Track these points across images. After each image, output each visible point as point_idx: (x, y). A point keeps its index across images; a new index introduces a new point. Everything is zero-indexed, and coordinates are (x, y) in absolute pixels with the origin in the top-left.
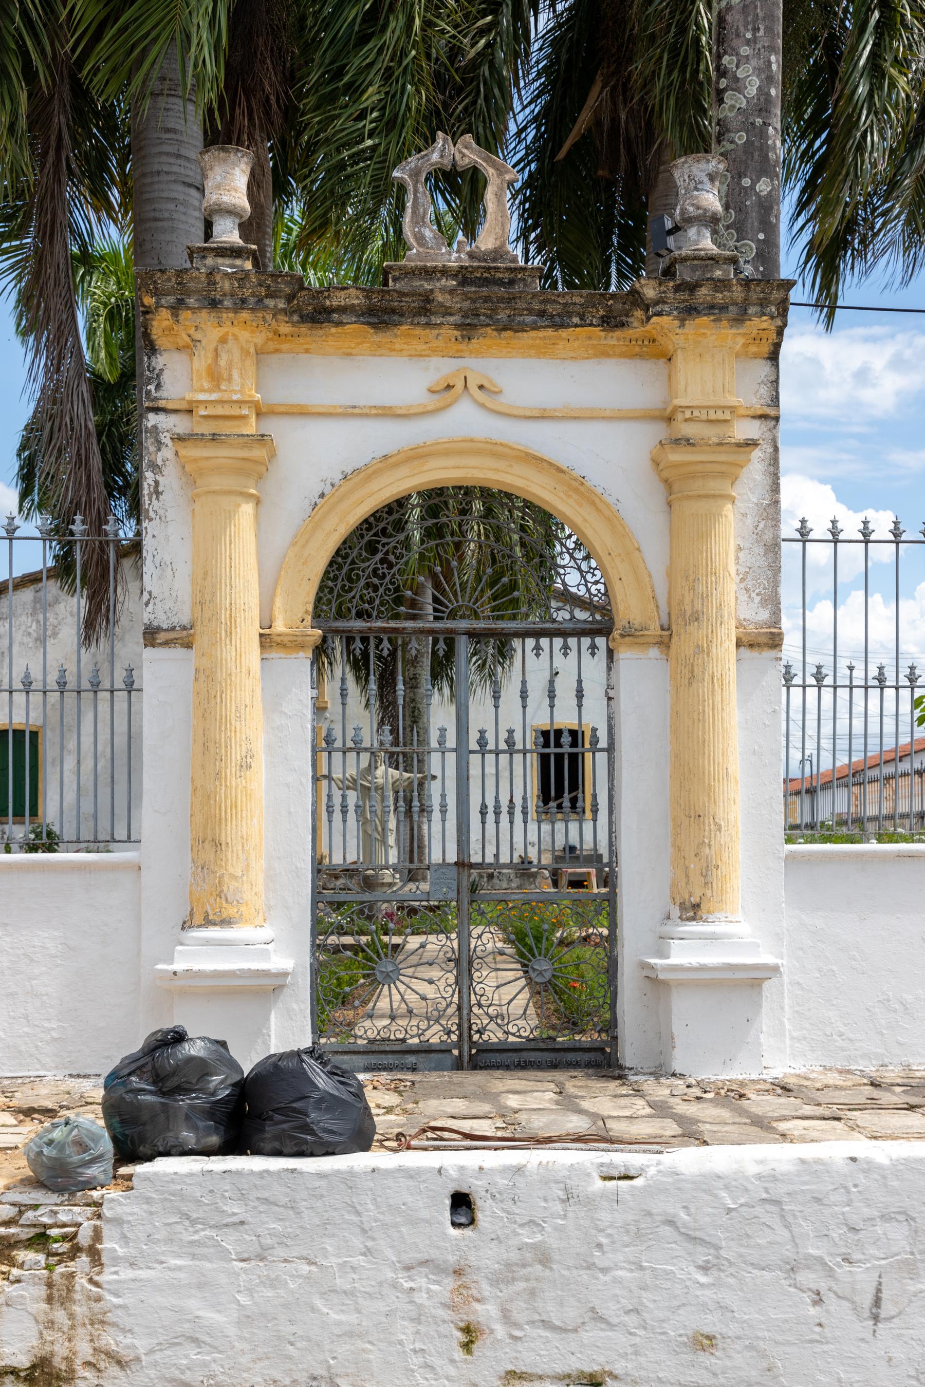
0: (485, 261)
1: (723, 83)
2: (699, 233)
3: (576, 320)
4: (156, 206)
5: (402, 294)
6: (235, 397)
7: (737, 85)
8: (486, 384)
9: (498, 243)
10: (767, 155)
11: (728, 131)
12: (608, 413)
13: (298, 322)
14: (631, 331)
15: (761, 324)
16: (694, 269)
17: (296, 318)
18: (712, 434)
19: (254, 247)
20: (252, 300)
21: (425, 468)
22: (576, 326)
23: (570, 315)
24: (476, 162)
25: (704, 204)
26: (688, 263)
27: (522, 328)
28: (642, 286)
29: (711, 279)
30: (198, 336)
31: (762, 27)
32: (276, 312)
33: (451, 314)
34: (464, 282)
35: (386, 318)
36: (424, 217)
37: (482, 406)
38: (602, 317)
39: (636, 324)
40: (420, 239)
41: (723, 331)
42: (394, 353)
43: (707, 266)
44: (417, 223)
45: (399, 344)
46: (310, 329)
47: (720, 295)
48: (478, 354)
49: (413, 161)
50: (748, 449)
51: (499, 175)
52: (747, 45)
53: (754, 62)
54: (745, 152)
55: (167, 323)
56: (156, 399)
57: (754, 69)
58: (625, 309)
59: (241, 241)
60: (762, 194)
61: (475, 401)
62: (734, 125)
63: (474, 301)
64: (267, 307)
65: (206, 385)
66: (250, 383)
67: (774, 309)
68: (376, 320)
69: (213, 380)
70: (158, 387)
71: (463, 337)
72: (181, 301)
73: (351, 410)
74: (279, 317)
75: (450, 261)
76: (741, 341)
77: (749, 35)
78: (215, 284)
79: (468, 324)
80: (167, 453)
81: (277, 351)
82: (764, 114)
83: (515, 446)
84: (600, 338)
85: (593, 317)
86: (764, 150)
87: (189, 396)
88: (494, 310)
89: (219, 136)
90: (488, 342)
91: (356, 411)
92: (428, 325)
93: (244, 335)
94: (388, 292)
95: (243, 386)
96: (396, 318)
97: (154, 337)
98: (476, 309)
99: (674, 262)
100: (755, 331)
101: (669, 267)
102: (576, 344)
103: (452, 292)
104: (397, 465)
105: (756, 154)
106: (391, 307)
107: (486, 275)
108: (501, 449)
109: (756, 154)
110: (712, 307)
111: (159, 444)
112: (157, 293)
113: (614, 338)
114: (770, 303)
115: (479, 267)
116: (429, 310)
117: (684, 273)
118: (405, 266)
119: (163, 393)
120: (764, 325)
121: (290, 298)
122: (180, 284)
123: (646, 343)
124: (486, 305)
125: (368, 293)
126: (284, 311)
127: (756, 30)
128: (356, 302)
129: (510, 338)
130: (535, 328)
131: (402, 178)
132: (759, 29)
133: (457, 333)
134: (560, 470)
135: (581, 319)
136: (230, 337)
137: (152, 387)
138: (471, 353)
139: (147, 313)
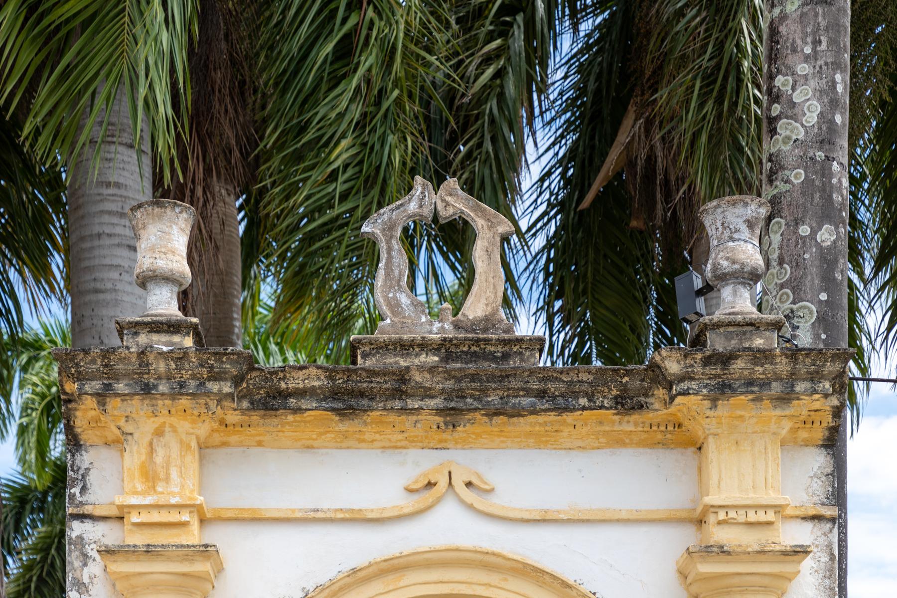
0: (474, 331)
1: (776, 109)
2: (735, 293)
3: (583, 401)
4: (97, 275)
5: (371, 373)
6: (173, 501)
7: (793, 110)
8: (475, 481)
9: (489, 309)
10: (831, 197)
11: (782, 168)
12: (624, 515)
13: (248, 409)
14: (651, 415)
15: (815, 404)
16: (729, 337)
17: (245, 404)
18: (750, 539)
19: (195, 320)
20: (193, 384)
21: (402, 584)
22: (584, 408)
23: (576, 395)
24: (462, 212)
25: (741, 257)
26: (722, 330)
27: (517, 413)
28: (663, 359)
29: (749, 349)
30: (129, 428)
31: (824, 39)
32: (222, 398)
33: (432, 397)
34: (448, 357)
35: (353, 402)
36: (399, 280)
37: (471, 507)
38: (616, 397)
39: (657, 406)
40: (395, 306)
41: (764, 413)
42: (363, 445)
43: (744, 333)
44: (391, 287)
45: (369, 433)
46: (263, 417)
47: (760, 369)
48: (464, 444)
49: (386, 213)
50: (796, 558)
51: (489, 228)
52: (806, 62)
53: (814, 83)
54: (803, 194)
55: (93, 413)
56: (81, 504)
57: (815, 91)
58: (642, 387)
59: (180, 314)
60: (825, 244)
61: (462, 502)
62: (789, 161)
63: (459, 380)
64: (208, 393)
65: (139, 487)
66: (192, 482)
67: (827, 385)
68: (341, 405)
69: (147, 480)
70: (84, 489)
71: (446, 423)
72: (108, 387)
73: (312, 515)
74: (225, 403)
75: (430, 332)
76: (787, 425)
77: (808, 50)
78: (148, 365)
79: (453, 409)
80: (95, 568)
81: (224, 444)
82: (827, 146)
83: (511, 556)
84: (613, 422)
85: (604, 397)
86: (827, 190)
87: (119, 500)
88: (484, 391)
89: (165, 191)
90: (477, 429)
91: (319, 515)
92: (404, 410)
93: (184, 426)
94: (355, 371)
95: (182, 486)
96: (365, 402)
97: (78, 430)
98: (461, 389)
99: (705, 327)
100: (805, 413)
101: (698, 336)
102: (585, 430)
103: (432, 370)
104: (367, 579)
105: (817, 196)
106: (359, 391)
107: (474, 348)
108: (493, 559)
109: (817, 196)
110: (750, 383)
111: (85, 556)
112: (80, 378)
113: (631, 424)
114: (823, 377)
115: (466, 339)
116: (405, 393)
117: (716, 343)
118: (377, 340)
119: (89, 497)
120: (817, 405)
121: (237, 380)
122: (106, 366)
123: (670, 428)
124: (474, 385)
125: (331, 374)
126: (230, 396)
127: (816, 42)
128: (317, 384)
129: (504, 423)
130: (534, 412)
131: (373, 234)
132: (820, 42)
133: (439, 419)
134: (565, 585)
135: (590, 400)
136: (167, 429)
137: (76, 490)
138: (457, 443)
139: (69, 401)
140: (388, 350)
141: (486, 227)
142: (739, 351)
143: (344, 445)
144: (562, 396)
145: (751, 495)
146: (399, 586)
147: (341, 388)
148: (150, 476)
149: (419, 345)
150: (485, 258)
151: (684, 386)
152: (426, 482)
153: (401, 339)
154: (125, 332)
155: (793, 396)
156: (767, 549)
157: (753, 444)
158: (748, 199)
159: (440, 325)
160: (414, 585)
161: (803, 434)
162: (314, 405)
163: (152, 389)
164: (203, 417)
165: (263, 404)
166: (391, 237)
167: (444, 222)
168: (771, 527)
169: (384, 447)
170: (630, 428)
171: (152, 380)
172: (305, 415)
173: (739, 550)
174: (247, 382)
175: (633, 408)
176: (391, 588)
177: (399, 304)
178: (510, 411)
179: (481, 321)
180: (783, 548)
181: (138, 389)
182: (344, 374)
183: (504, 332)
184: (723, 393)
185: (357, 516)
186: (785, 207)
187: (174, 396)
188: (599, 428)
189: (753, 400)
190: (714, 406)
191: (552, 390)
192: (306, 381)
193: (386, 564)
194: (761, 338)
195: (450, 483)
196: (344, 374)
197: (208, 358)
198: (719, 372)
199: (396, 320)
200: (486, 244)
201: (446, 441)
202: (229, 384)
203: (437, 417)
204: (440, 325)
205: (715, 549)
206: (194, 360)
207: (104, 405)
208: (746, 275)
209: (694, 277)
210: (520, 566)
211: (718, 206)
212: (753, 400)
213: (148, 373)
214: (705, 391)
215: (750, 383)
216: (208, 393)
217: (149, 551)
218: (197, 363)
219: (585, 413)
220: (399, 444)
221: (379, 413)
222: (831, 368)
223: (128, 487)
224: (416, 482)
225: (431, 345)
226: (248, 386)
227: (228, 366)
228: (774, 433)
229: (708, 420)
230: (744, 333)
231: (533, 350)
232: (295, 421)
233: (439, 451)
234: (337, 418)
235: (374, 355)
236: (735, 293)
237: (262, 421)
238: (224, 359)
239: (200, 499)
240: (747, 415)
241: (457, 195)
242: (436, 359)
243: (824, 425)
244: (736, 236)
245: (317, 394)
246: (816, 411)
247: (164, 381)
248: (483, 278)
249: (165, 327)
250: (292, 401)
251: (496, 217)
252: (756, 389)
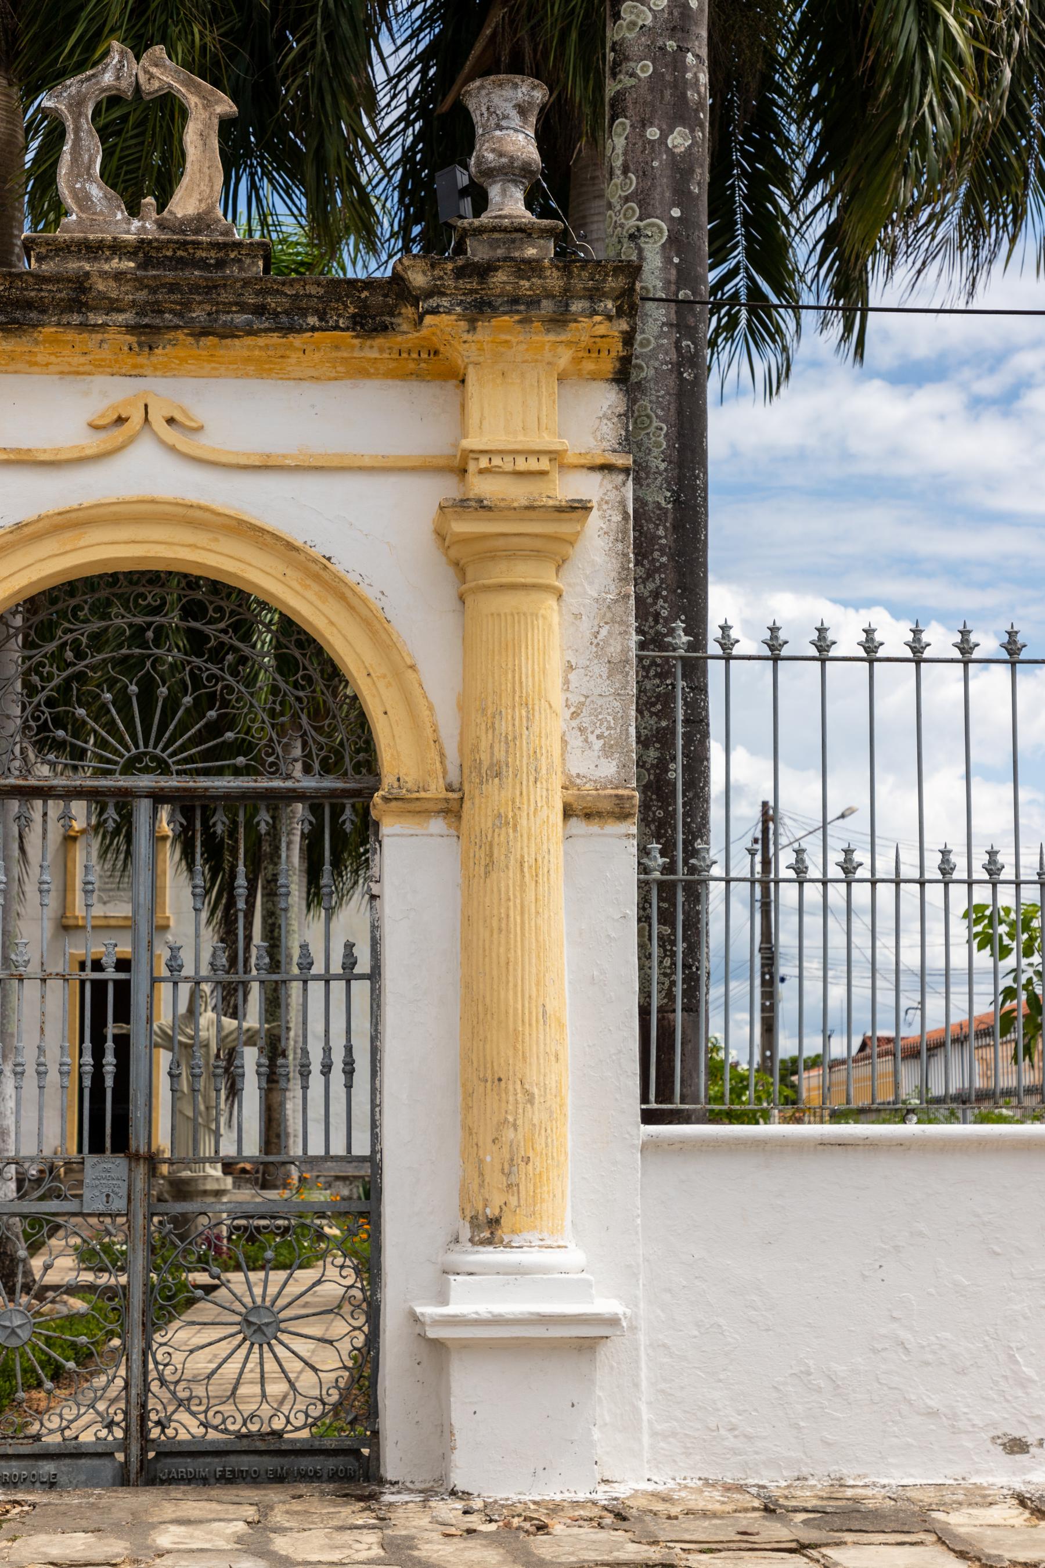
2: (504, 192)
3: (313, 320)
8: (178, 416)
14: (399, 339)
16: (493, 245)
18: (518, 492)
21: (82, 543)
22: (313, 329)
23: (304, 313)
24: (170, 86)
25: (510, 148)
26: (485, 236)
36: (89, 168)
37: (172, 449)
38: (354, 316)
39: (405, 327)
40: (84, 200)
41: (535, 338)
42: (35, 369)
43: (513, 241)
44: (79, 175)
48: (165, 370)
49: (73, 85)
51: (205, 107)
58: (386, 305)
61: (162, 442)
75: (128, 232)
83: (221, 511)
85: (339, 316)
100: (585, 338)
102: (317, 356)
104: (38, 537)
107: (180, 253)
108: (198, 514)
113: (373, 350)
114: (605, 295)
115: (169, 241)
117: (478, 251)
120: (601, 330)
129: (214, 346)
130: (251, 332)
131: (56, 109)
135: (321, 319)
138: (156, 369)
140: (70, 252)
141: (200, 106)
142: (498, 260)
143: (10, 368)
144: (286, 313)
145: (521, 438)
149: (110, 247)
150: (199, 143)
151: (433, 302)
152: (115, 417)
155: (569, 317)
156: (536, 504)
157: (523, 375)
158: (517, 79)
159: (140, 224)
161: (589, 366)
166: (80, 115)
167: (148, 98)
168: (546, 478)
169: (62, 373)
170: (374, 354)
173: (502, 504)
175: (375, 330)
176: (68, 548)
177: (88, 197)
178: (221, 330)
179: (192, 220)
180: (557, 503)
183: (222, 234)
184: (482, 312)
185: (25, 458)
186: (630, 105)
188: (334, 354)
189: (520, 322)
190: (472, 329)
191: (273, 305)
194: (534, 247)
195: (146, 419)
198: (475, 286)
199: (84, 216)
200: (201, 126)
201: (142, 367)
204: (140, 224)
205: (473, 504)
208: (517, 172)
209: (458, 174)
210: (234, 523)
211: (482, 87)
212: (520, 322)
214: (458, 309)
215: (515, 301)
219: (316, 334)
220: (81, 369)
222: (612, 283)
224: (102, 416)
228: (549, 363)
229: (467, 345)
230: (513, 241)
231: (255, 256)
233: (132, 379)
235: (52, 259)
236: (504, 192)
240: (514, 340)
241: (164, 66)
242: (132, 264)
243: (614, 354)
244: (504, 123)
246: (602, 337)
248: (196, 167)
251: (213, 94)
252: (522, 308)
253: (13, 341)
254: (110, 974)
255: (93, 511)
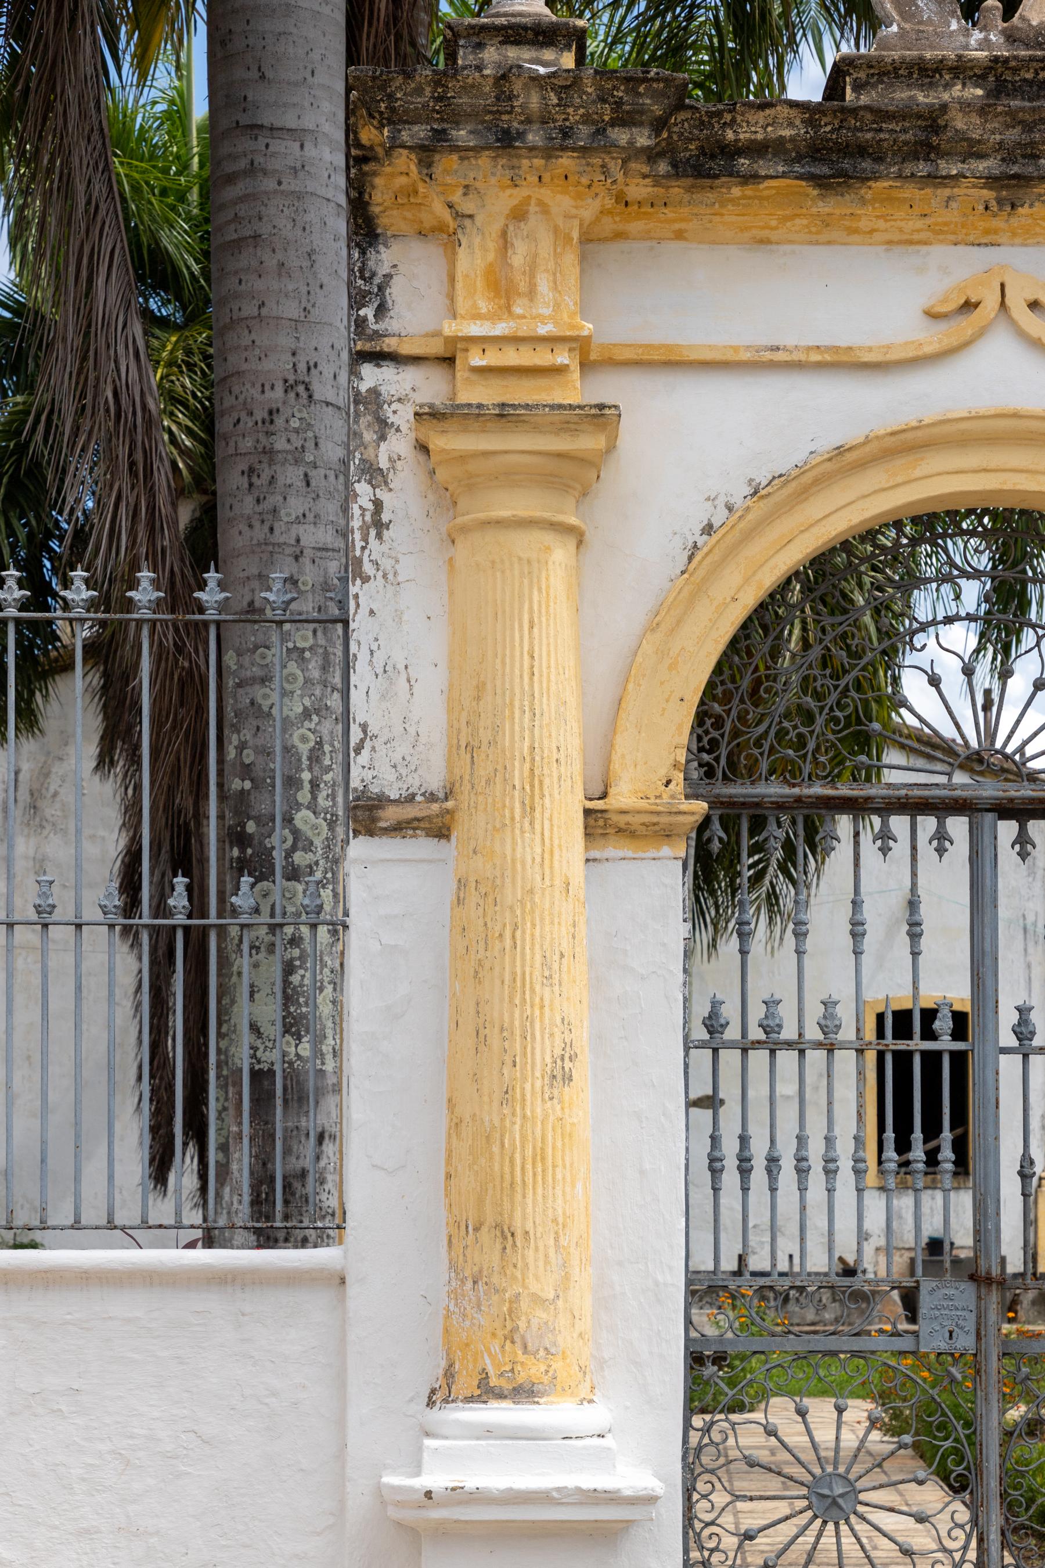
6: (543, 330)
13: (667, 176)
17: (663, 167)
21: (918, 473)
30: (467, 206)
34: (999, 90)
35: (846, 164)
45: (868, 217)
61: (1022, 335)
65: (484, 306)
66: (570, 301)
68: (825, 170)
69: (497, 293)
87: (450, 328)
93: (561, 202)
104: (861, 465)
115: (1032, 59)
128: (787, 133)
133: (988, 194)
136: (533, 208)
138: (1014, 234)
143: (823, 237)
146: (913, 476)
147: (827, 141)
148: (503, 289)
149: (951, 69)
152: (962, 301)
153: (921, 58)
154: (462, 42)
160: (939, 474)
162: (780, 169)
163: (515, 139)
164: (596, 188)
165: (693, 167)
169: (890, 242)
171: (515, 124)
172: (761, 186)
174: (669, 131)
176: (899, 479)
181: (492, 138)
182: (835, 116)
185: (845, 358)
187: (549, 153)
192: (770, 129)
193: (893, 439)
195: (1003, 303)
196: (835, 116)
197: (614, 88)
201: (996, 232)
202: (646, 132)
203: (985, 192)
206: (589, 90)
207: (429, 165)
213: (510, 113)
216: (611, 147)
217: (505, 415)
218: (594, 96)
220: (916, 237)
221: (886, 184)
223: (462, 305)
224: (945, 301)
225: (972, 68)
226: (670, 137)
227: (648, 101)
232: (744, 197)
233: (982, 249)
234: (816, 192)
237: (687, 197)
238: (641, 90)
239: (587, 328)
242: (980, 92)
245: (786, 152)
247: (535, 127)
249: (530, 35)
250: (743, 163)
253: (832, 200)
254: (946, 1043)
255: (935, 430)
